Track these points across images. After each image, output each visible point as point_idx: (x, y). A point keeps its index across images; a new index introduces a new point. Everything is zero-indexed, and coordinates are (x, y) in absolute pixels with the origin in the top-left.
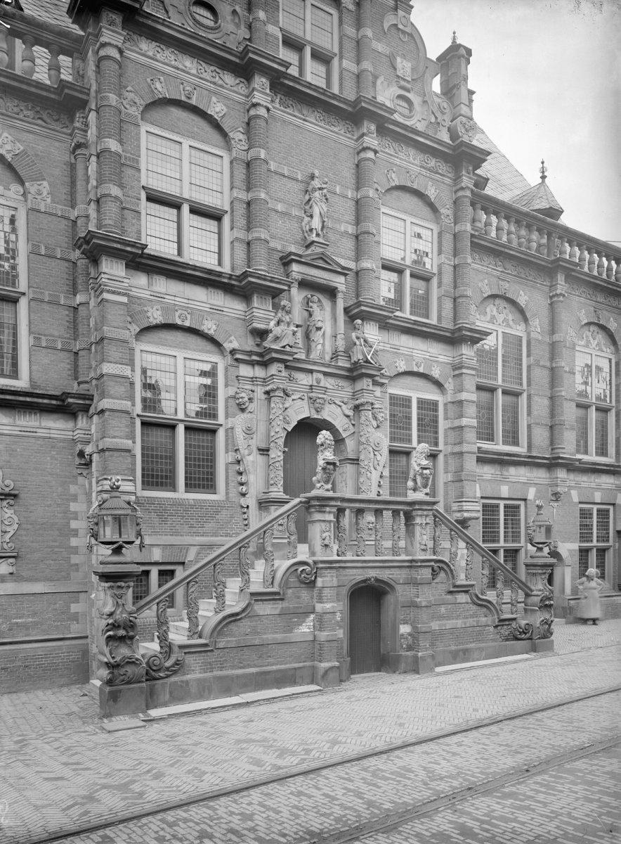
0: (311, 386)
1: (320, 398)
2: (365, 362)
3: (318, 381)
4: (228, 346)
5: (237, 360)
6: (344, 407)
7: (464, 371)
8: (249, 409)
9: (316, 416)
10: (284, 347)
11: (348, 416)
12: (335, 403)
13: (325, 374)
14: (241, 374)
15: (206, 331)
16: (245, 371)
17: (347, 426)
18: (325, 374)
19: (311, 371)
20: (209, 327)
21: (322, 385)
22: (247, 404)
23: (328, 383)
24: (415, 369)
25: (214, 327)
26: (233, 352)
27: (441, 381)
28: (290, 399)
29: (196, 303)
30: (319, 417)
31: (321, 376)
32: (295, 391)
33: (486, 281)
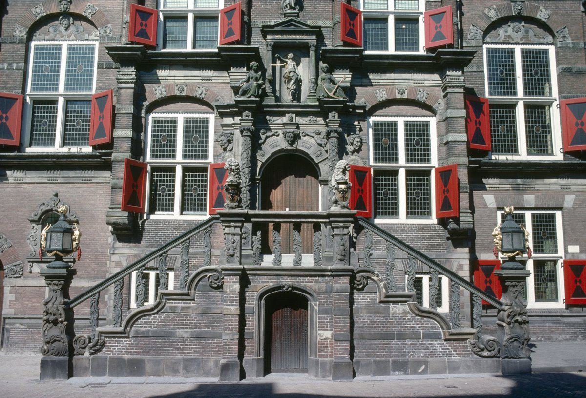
0: (283, 124)
1: (288, 133)
2: (326, 97)
4: (214, 104)
6: (316, 137)
7: (449, 90)
9: (289, 148)
10: (249, 97)
11: (320, 145)
12: (308, 135)
15: (198, 96)
16: (228, 120)
17: (319, 153)
18: (298, 114)
19: (282, 114)
21: (294, 121)
22: (226, 145)
24: (398, 96)
25: (204, 92)
26: (218, 107)
27: (428, 102)
29: (190, 78)
31: (294, 115)
33: (495, 7)
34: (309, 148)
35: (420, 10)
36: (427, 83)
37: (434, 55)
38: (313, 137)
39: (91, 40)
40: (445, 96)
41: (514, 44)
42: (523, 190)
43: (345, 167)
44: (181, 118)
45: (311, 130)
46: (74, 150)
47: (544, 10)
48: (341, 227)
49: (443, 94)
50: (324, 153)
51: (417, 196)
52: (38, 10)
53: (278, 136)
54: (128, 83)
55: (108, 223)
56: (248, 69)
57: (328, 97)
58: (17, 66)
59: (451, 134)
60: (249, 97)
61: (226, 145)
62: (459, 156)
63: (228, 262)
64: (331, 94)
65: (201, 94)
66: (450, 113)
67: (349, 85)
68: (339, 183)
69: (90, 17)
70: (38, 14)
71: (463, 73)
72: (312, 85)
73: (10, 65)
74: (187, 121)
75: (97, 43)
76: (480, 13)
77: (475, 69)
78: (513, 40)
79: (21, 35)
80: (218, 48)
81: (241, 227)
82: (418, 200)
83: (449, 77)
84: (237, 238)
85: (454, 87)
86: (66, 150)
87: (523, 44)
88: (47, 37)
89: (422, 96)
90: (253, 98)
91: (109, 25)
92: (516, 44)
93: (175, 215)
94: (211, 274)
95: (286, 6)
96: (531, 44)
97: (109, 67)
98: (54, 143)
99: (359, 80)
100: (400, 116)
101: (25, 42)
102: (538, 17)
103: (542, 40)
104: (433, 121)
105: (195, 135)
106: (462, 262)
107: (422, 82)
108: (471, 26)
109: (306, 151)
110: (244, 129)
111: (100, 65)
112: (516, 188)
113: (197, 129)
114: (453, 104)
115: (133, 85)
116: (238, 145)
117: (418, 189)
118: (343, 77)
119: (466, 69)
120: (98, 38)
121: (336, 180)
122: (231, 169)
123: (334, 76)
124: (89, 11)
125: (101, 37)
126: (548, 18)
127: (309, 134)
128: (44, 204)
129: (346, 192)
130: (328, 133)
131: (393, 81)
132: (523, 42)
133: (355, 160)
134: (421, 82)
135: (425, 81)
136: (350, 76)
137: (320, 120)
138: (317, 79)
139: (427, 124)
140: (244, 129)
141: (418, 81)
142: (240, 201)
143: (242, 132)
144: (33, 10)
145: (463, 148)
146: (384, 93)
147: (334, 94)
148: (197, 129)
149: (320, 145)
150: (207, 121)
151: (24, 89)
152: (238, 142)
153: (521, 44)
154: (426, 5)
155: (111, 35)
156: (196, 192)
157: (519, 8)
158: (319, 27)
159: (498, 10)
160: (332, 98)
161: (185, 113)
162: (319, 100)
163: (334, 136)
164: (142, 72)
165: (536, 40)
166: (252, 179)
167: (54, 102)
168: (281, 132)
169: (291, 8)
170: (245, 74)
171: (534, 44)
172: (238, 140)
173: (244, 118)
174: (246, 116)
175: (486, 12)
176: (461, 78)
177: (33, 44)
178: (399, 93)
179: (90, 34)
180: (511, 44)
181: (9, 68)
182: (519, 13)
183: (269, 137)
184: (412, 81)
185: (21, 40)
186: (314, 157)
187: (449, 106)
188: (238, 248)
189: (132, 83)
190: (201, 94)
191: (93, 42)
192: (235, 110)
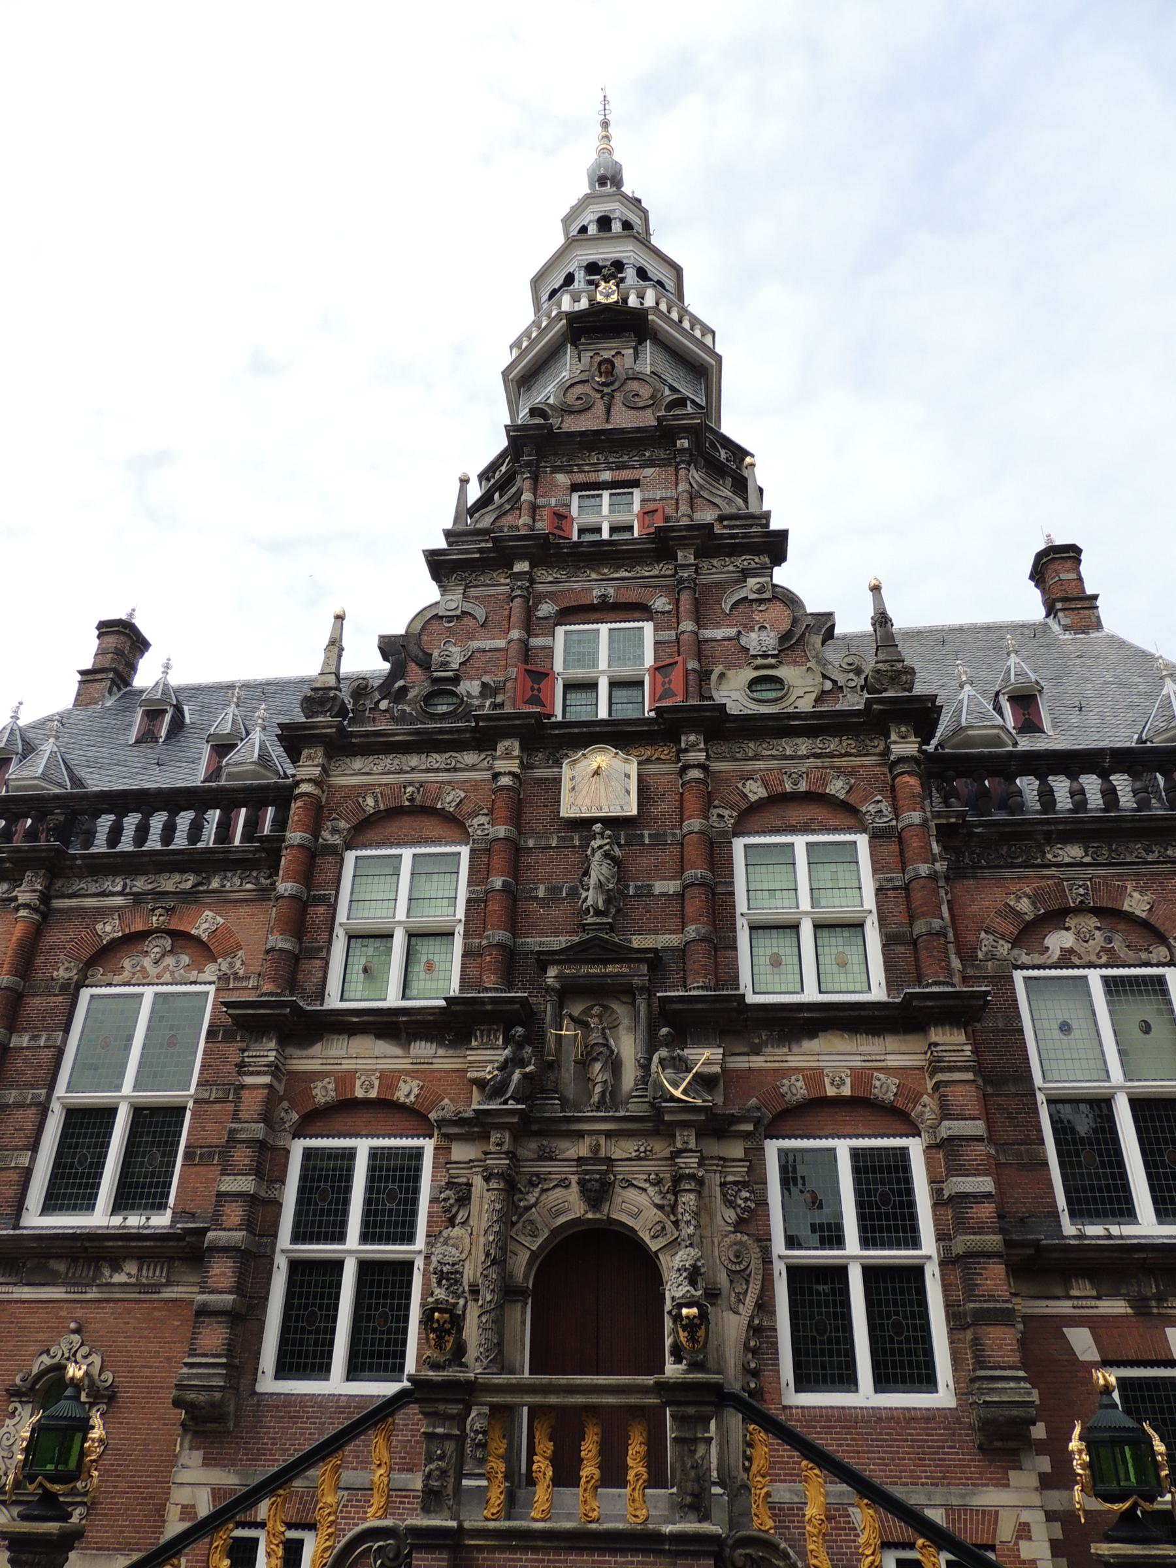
0: (580, 1159)
2: (666, 1101)
3: (596, 1149)
5: (446, 1136)
6: (651, 1191)
8: (458, 1220)
9: (590, 1216)
12: (633, 1185)
13: (609, 1134)
14: (454, 1158)
15: (402, 1100)
16: (461, 1152)
18: (609, 1134)
19: (580, 1135)
20: (407, 1091)
21: (602, 1154)
22: (454, 1210)
23: (623, 1149)
26: (441, 1122)
27: (899, 1105)
28: (538, 1190)
30: (598, 1216)
31: (602, 1141)
32: (550, 1173)
34: (636, 1216)
35: (866, 907)
36: (894, 1061)
37: (898, 1000)
38: (645, 1190)
39: (200, 983)
40: (937, 1086)
41: (1084, 967)
42: (1160, 1314)
43: (694, 1266)
44: (363, 1147)
45: (639, 1173)
46: (134, 1221)
47: (1136, 895)
48: (691, 1417)
49: (930, 1085)
50: (669, 1226)
51: (897, 1334)
52: (108, 928)
53: (567, 1187)
54: (258, 1073)
55: (177, 1403)
56: (506, 1043)
57: (673, 1099)
58: (48, 1039)
59: (954, 1179)
60: (505, 1103)
61: (454, 1210)
62: (979, 1230)
63: (426, 1510)
64: (677, 1093)
65: (408, 1096)
66: (948, 1128)
67: (719, 1070)
68: (680, 1306)
69: (204, 937)
70: (108, 934)
71: (972, 1037)
72: (640, 1073)
73: (34, 1038)
74: (375, 1154)
75: (212, 989)
76: (999, 906)
77: (1001, 1025)
78: (1080, 958)
79: (67, 976)
80: (445, 999)
81: (461, 1419)
82: (900, 1342)
83: (939, 1048)
84: (450, 1447)
85: (951, 1069)
86: (117, 1221)
87: (1106, 966)
88: (117, 979)
89: (884, 1090)
90: (512, 1105)
91: (240, 953)
92: (1089, 967)
93: (337, 1383)
94: (381, 1543)
95: (588, 909)
96: (1123, 966)
97: (229, 1037)
98: (94, 1204)
99: (745, 1058)
100: (839, 1137)
101: (71, 991)
102: (1126, 907)
103: (1144, 956)
104: (916, 1148)
105: (390, 1186)
106: (1025, 1517)
107: (882, 1057)
108: (983, 935)
109: (630, 1222)
110: (491, 1174)
111: (211, 1034)
112: (1141, 1306)
113: (395, 1177)
114: (955, 1109)
115: (266, 1079)
116: (480, 1211)
117: (896, 1313)
118: (705, 1057)
119: (978, 1026)
120: (215, 978)
121: (673, 1299)
122: (442, 1271)
123: (686, 1051)
124: (206, 926)
125: (224, 978)
126: (1150, 910)
127: (635, 1182)
128: (48, 1352)
129: (699, 1326)
130: (677, 1179)
131: (816, 1058)
132: (1104, 959)
133: (740, 1243)
134: (878, 1058)
135: (888, 1057)
136: (721, 1051)
137: (661, 1148)
138: (650, 1060)
139: (904, 1153)
140: (491, 1174)
141: (873, 1058)
142: (460, 1349)
143: (487, 1179)
144: (99, 927)
145: (986, 1211)
146: (799, 1084)
147: (685, 1092)
148: (395, 1177)
149: (660, 1207)
150: (418, 1153)
151: (51, 1087)
152: (481, 1206)
153: (1101, 967)
154: (876, 895)
155: (241, 972)
156: (386, 1322)
157: (1081, 891)
158: (655, 951)
159: (1035, 899)
160: (680, 1100)
161: (373, 1136)
162: (652, 1105)
163: (687, 1187)
164: (290, 1051)
165: (1131, 956)
166: (509, 1292)
167: (112, 1112)
168: (574, 1179)
169: (598, 913)
170: (499, 1052)
171: (1129, 966)
172: (481, 1198)
173: (493, 1148)
174: (498, 1145)
175: (1012, 903)
176: (965, 1048)
177: (85, 994)
178: (832, 1084)
179: (201, 971)
180: (1078, 967)
181: (32, 1042)
182: (1082, 902)
183: (548, 1190)
184: (858, 1058)
185: (65, 987)
186: (646, 1237)
187: (946, 1113)
188: (451, 1473)
189: (265, 1073)
190: (408, 1096)
191: (205, 989)
192: (475, 1127)
